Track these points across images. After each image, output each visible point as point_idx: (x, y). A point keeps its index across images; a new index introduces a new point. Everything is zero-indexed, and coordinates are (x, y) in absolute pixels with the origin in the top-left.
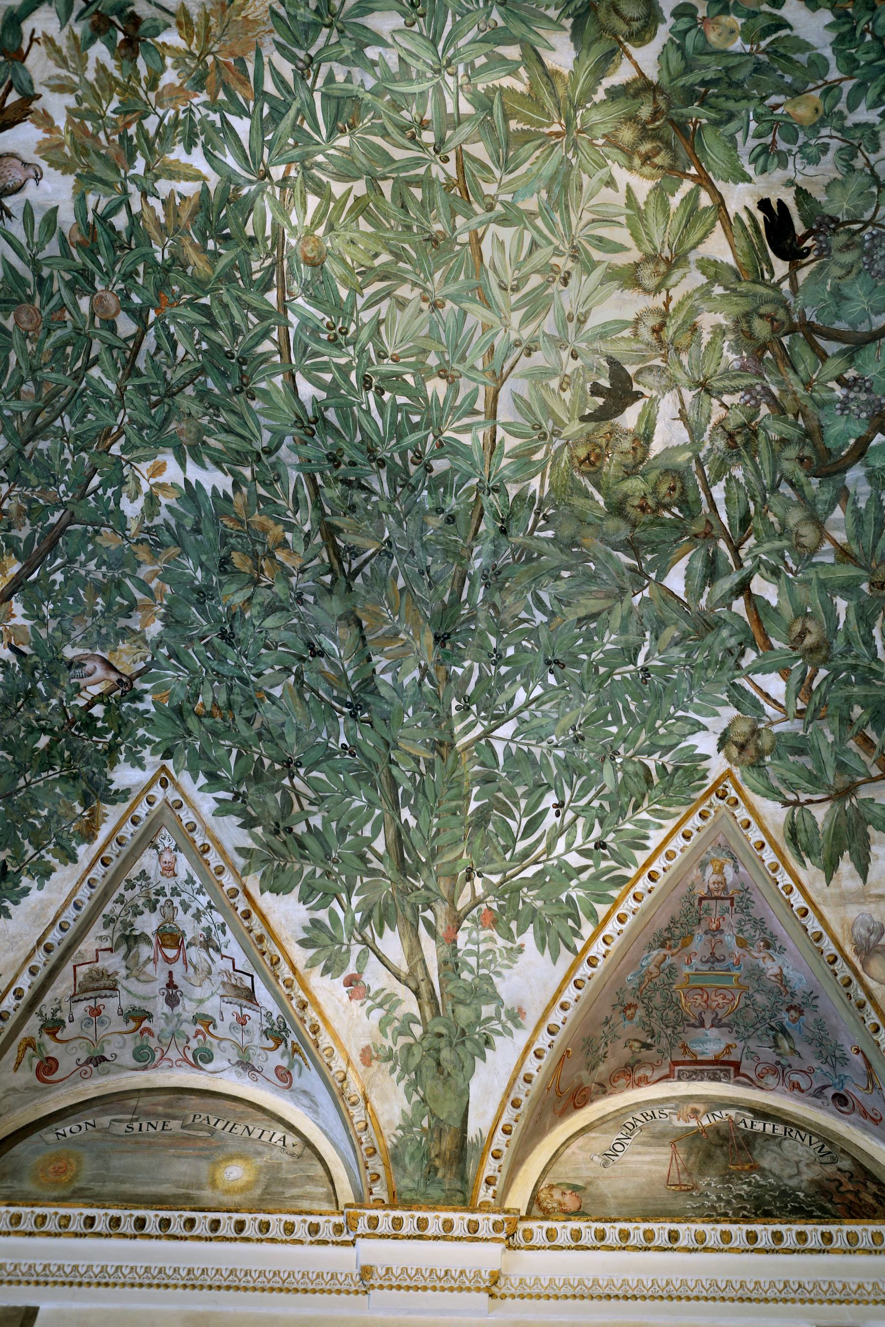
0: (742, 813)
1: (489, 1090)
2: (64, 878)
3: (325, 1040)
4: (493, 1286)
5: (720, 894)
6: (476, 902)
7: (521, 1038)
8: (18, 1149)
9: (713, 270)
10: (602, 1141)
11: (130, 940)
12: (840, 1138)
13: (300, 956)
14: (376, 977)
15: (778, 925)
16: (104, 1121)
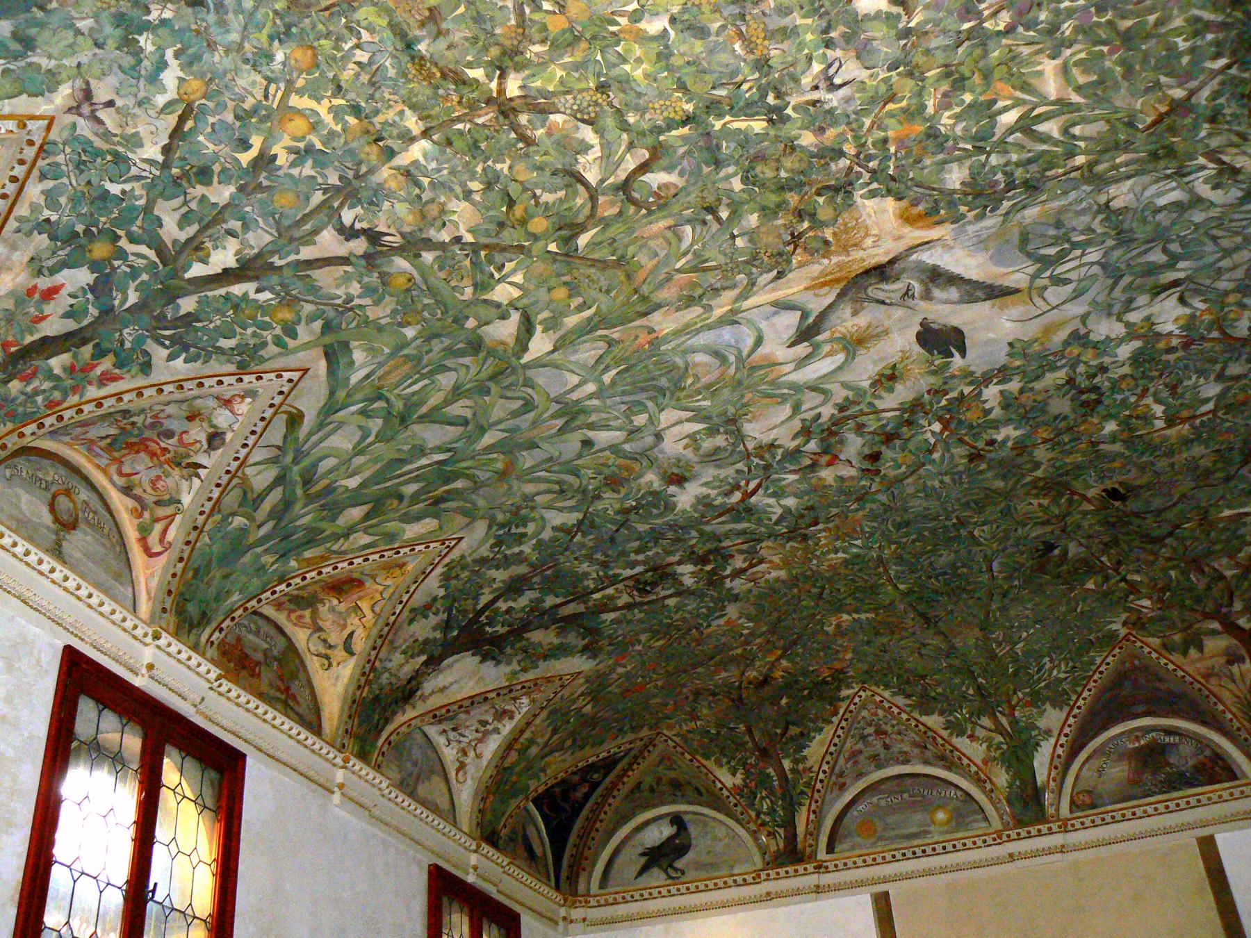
0: (1139, 644)
1: (1041, 762)
2: (829, 730)
3: (965, 761)
4: (1062, 849)
5: (1134, 669)
6: (1020, 700)
7: (1053, 741)
8: (846, 820)
9: (1087, 513)
10: (1097, 763)
11: (863, 738)
12: (1205, 738)
13: (945, 734)
14: (981, 733)
15: (1163, 673)
16: (875, 800)
